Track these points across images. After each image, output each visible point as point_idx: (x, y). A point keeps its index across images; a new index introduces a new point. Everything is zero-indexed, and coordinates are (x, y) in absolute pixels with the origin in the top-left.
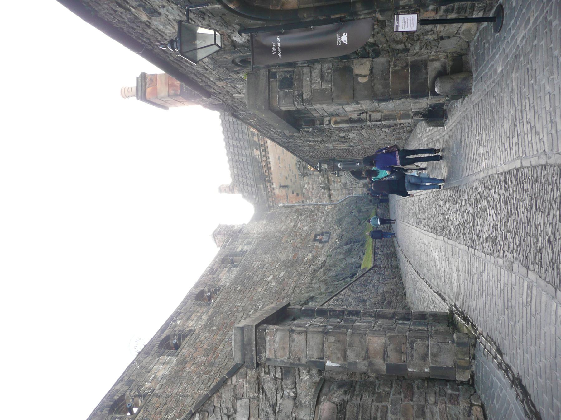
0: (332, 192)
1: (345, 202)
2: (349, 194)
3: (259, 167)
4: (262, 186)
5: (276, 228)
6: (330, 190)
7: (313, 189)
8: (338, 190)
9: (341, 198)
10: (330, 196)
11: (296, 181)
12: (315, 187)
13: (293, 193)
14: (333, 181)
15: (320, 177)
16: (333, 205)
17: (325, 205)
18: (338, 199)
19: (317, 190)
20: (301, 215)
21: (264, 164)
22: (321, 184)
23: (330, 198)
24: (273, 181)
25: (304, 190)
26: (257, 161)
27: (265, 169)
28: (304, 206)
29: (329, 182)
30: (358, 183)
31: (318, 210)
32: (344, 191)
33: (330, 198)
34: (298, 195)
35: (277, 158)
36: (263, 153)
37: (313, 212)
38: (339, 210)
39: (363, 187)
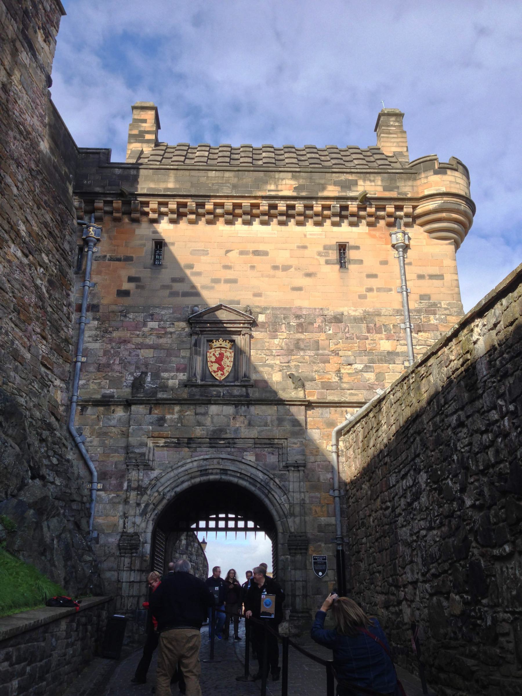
0: (120, 413)
1: (71, 456)
2: (103, 476)
3: (235, 187)
4: (171, 185)
5: (19, 165)
6: (128, 404)
7: (141, 346)
8: (126, 435)
9: (92, 444)
10: (106, 402)
11: (174, 294)
12: (146, 354)
13: (131, 279)
14: (161, 421)
15: (182, 376)
16: (68, 408)
17: (70, 380)
18: (87, 432)
19: (134, 360)
20: (50, 282)
21: (246, 203)
22: (156, 376)
23: (97, 403)
24: (183, 224)
25: (140, 317)
26: (259, 184)
27: (229, 204)
28: (79, 309)
29: (159, 403)
30: (144, 513)
31: (57, 349)
32: (119, 457)
33: (97, 403)
34: (123, 294)
35: (262, 247)
36: (282, 206)
37: (57, 329)
38: (50, 427)
39: (124, 534)
